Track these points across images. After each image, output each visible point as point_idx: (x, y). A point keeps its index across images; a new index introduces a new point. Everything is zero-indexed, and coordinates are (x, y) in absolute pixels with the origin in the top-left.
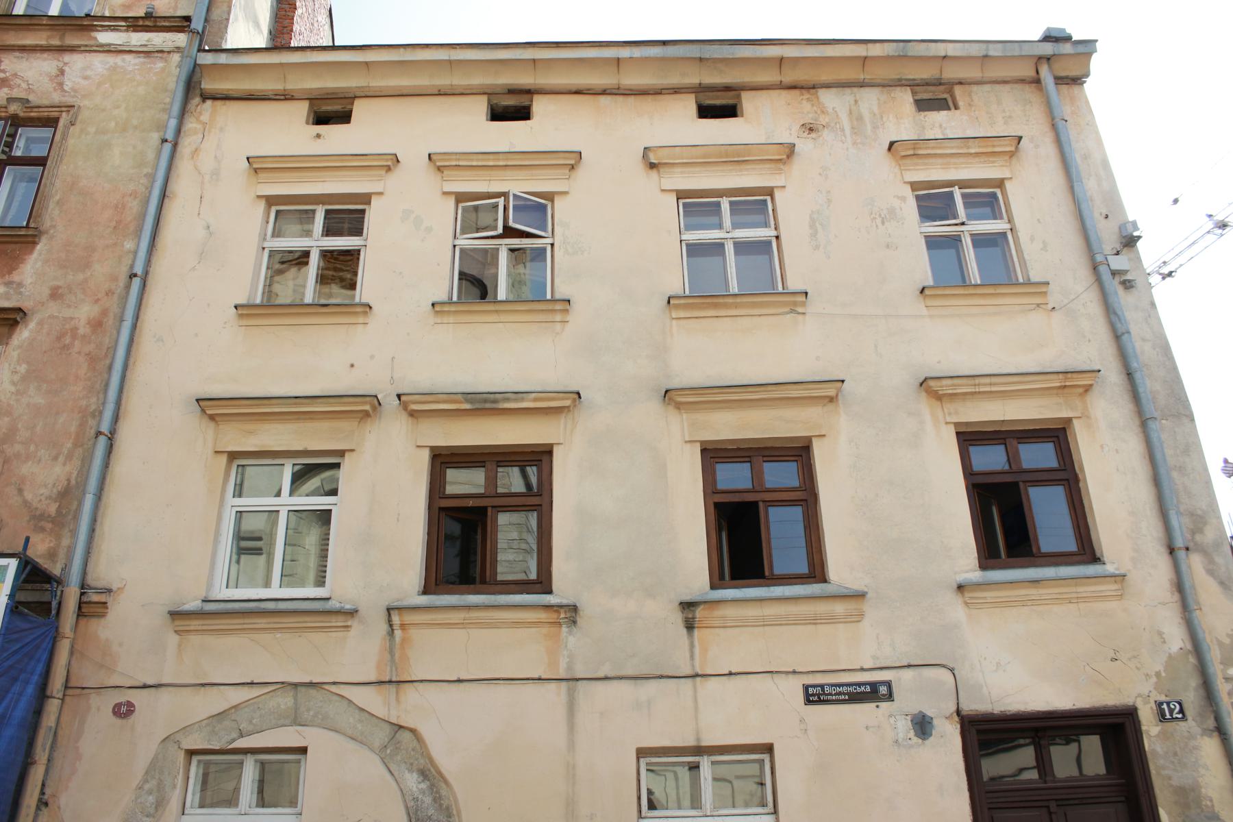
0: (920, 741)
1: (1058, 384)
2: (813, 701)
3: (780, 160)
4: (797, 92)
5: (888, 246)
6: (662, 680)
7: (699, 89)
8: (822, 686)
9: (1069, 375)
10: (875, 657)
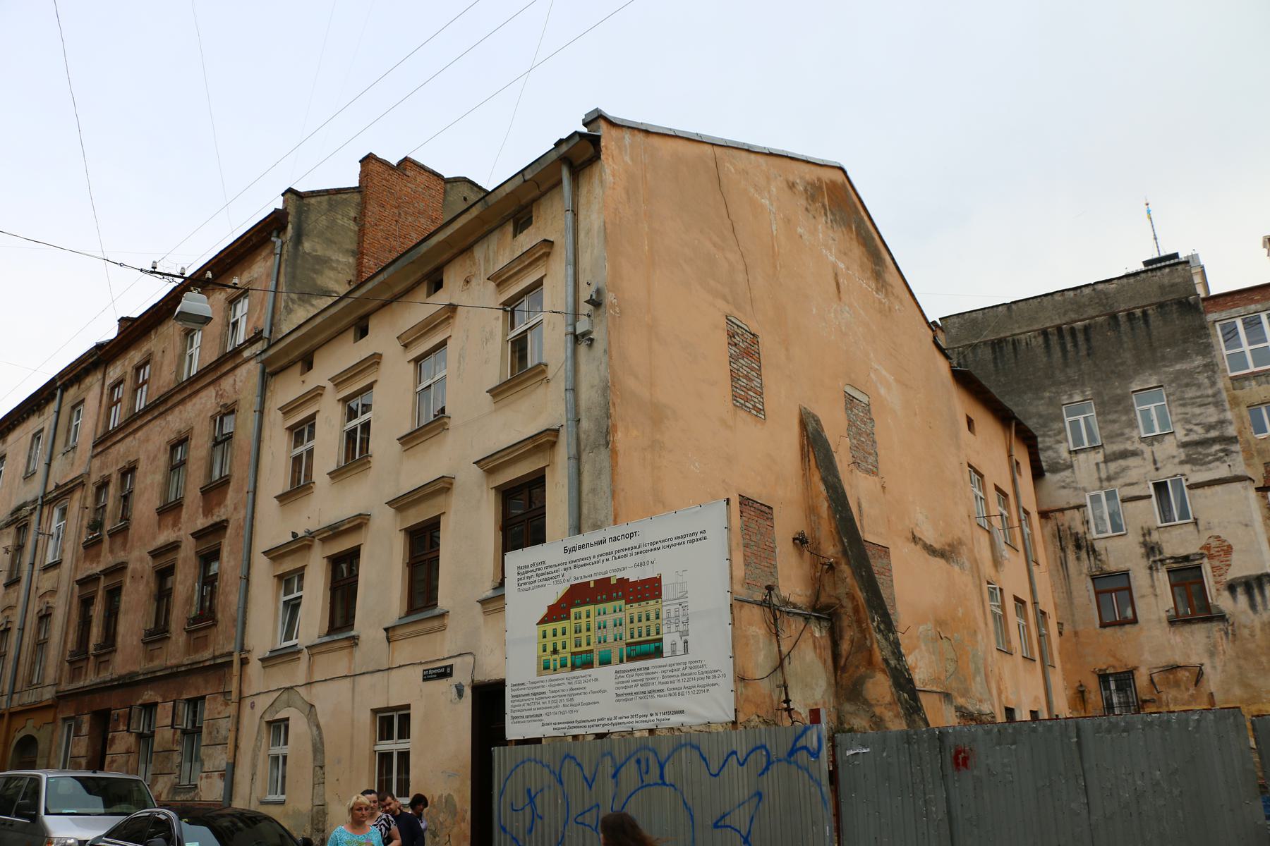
8: (428, 670)
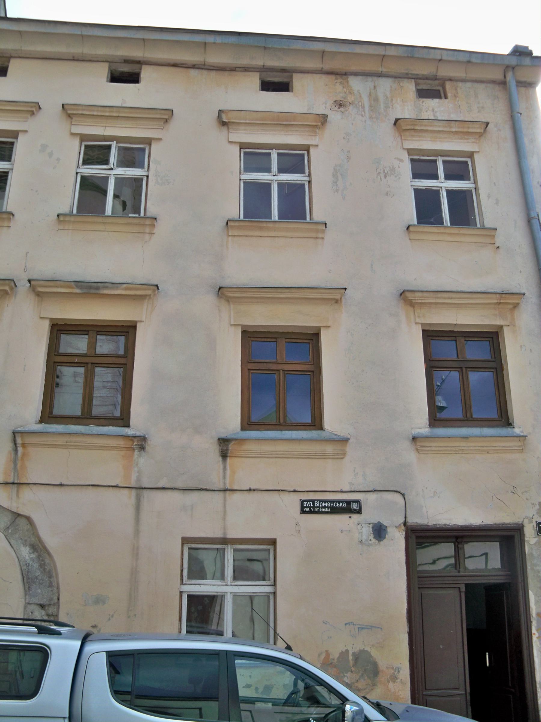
0: (377, 542)
1: (496, 301)
2: (306, 511)
3: (316, 126)
4: (333, 77)
5: (387, 194)
6: (203, 492)
7: (263, 70)
8: (313, 502)
9: (504, 296)
10: (351, 484)
